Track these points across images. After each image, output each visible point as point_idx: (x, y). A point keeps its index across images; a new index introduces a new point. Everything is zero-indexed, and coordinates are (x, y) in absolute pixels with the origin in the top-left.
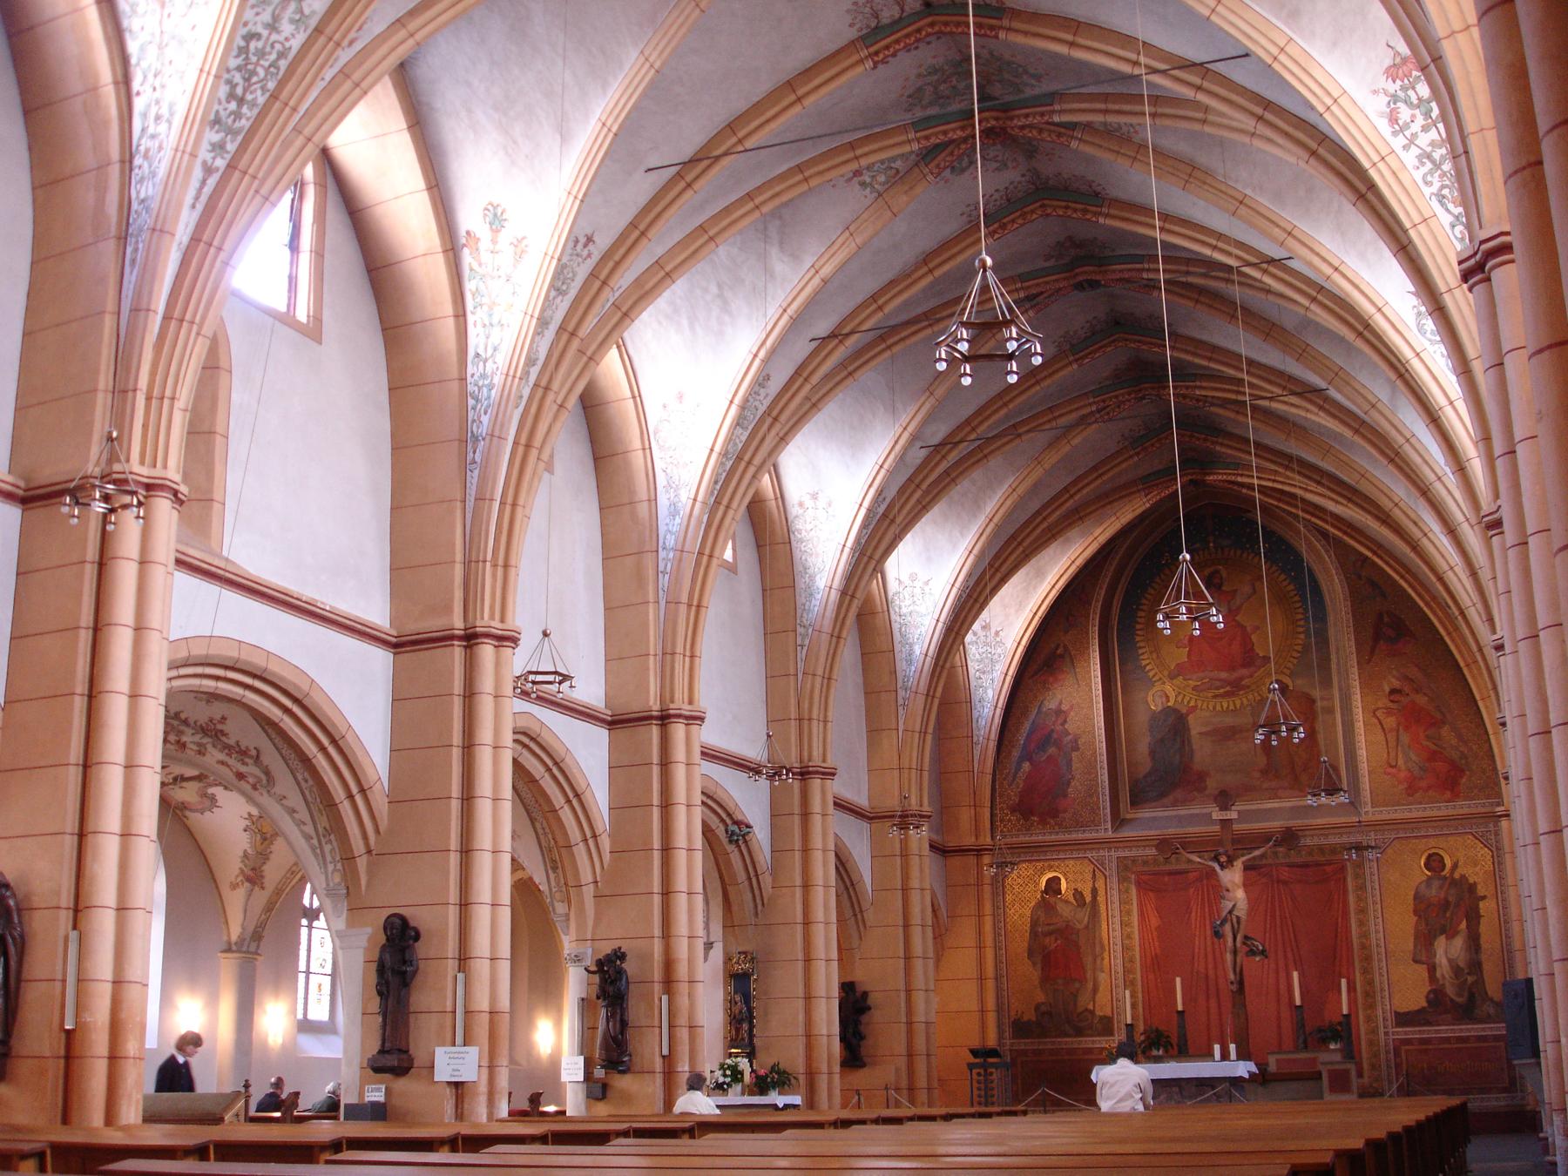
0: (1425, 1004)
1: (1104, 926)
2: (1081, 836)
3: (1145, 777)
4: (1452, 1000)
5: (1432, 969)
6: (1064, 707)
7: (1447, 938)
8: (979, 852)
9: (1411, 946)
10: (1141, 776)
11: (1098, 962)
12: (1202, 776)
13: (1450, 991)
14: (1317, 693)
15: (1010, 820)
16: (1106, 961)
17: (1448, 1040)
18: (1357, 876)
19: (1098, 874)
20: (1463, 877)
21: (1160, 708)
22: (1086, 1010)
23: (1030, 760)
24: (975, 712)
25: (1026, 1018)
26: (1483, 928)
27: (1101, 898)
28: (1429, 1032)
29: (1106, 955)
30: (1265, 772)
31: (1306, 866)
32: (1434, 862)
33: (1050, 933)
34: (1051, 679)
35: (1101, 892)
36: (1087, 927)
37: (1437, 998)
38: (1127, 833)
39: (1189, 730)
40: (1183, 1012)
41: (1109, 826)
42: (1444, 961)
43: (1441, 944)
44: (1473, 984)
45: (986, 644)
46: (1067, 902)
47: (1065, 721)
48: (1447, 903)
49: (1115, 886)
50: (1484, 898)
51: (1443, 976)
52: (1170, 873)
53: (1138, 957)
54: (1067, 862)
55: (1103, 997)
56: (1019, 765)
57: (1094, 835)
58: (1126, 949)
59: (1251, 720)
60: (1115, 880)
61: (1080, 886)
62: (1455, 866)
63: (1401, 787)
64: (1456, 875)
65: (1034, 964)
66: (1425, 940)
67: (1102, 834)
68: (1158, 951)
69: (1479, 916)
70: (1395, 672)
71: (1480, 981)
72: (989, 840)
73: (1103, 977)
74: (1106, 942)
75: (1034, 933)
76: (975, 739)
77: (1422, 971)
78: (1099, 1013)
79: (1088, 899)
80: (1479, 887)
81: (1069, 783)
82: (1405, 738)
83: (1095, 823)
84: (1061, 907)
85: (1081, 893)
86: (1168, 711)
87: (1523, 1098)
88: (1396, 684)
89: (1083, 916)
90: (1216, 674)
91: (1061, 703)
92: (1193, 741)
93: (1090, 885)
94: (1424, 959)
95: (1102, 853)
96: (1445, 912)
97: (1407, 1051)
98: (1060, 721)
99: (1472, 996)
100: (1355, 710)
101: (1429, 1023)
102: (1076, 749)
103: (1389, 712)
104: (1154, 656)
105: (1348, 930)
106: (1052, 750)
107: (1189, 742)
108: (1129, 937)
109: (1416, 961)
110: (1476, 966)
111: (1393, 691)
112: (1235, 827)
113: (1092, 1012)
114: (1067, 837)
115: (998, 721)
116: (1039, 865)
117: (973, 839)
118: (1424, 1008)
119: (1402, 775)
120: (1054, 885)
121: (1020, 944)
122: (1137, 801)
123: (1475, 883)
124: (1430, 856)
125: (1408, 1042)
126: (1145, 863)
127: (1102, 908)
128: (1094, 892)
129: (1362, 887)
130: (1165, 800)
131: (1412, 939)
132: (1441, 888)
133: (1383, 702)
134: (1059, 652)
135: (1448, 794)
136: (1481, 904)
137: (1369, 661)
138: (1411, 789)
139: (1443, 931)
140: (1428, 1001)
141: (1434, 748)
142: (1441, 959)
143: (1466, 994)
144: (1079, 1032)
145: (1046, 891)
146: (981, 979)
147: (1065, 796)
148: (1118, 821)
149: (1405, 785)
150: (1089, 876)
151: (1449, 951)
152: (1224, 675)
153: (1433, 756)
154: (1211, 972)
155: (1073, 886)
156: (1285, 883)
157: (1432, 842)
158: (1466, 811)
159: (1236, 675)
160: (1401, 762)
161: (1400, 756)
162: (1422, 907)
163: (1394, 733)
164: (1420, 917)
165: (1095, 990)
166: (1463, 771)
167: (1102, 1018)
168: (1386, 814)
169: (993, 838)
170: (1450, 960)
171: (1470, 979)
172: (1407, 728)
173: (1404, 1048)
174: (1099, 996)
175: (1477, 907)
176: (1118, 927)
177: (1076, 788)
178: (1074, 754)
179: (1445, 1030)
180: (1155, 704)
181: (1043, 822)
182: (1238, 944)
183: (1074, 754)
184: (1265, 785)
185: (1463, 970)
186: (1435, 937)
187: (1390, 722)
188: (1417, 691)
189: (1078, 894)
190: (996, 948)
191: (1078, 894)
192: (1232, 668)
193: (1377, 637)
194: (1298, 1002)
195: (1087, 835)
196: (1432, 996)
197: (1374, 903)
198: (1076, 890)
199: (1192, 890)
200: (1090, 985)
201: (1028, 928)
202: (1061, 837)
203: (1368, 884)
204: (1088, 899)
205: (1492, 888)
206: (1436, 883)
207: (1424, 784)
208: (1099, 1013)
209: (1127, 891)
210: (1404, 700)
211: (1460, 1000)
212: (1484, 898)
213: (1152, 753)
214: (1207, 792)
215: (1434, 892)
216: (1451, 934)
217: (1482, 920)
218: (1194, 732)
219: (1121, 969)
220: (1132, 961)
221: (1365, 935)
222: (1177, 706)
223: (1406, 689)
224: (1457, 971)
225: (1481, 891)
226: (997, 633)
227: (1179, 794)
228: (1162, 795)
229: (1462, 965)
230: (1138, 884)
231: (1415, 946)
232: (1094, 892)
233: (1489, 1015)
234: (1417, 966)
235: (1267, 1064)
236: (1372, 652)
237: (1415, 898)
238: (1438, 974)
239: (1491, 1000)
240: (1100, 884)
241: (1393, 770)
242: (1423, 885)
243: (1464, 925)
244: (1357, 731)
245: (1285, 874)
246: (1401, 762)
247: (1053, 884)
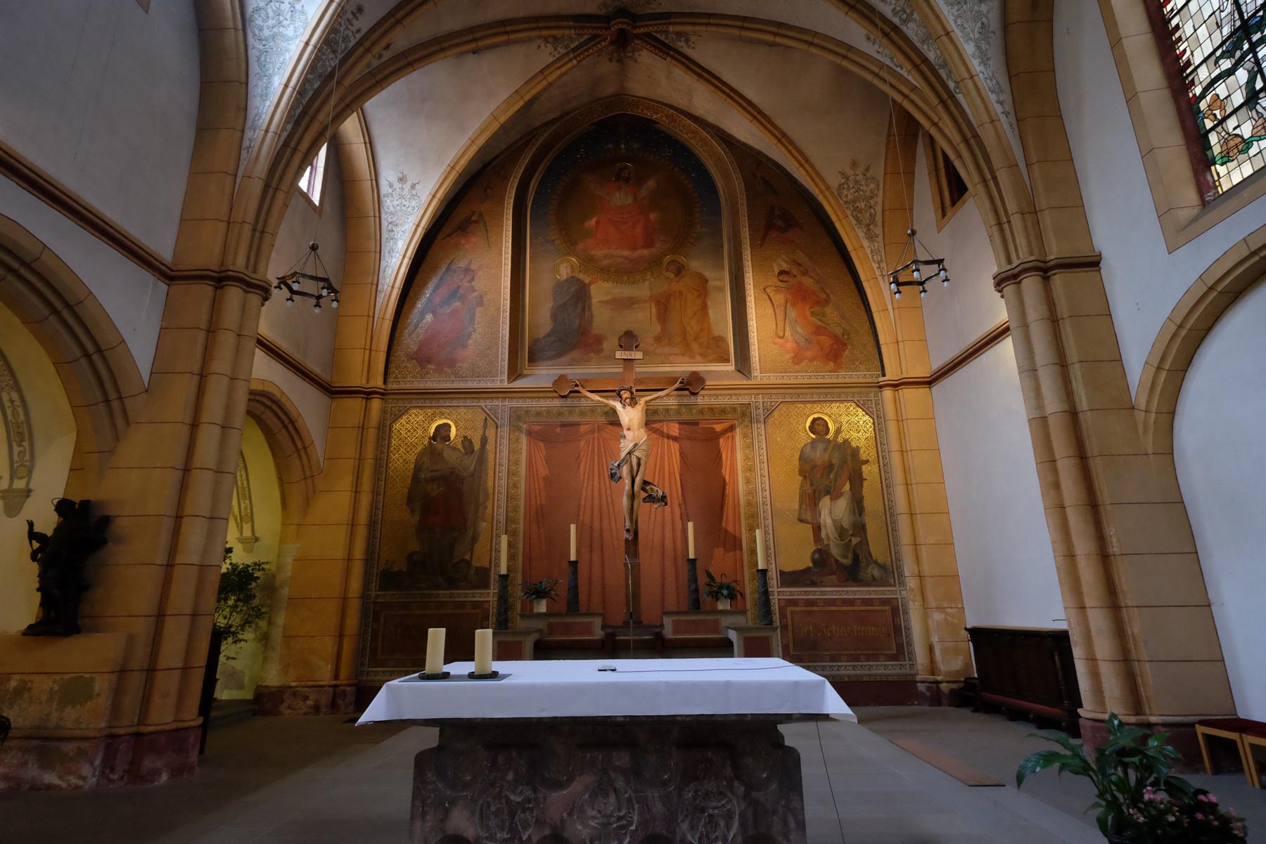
0: (811, 565)
1: (491, 473)
2: (475, 385)
3: (544, 337)
4: (837, 561)
5: (817, 529)
6: (473, 267)
7: (831, 499)
8: (368, 394)
9: (796, 505)
10: (541, 336)
11: (481, 511)
12: (599, 340)
13: (835, 551)
14: (707, 274)
15: (406, 367)
16: (489, 511)
17: (833, 602)
18: (745, 436)
19: (490, 422)
20: (846, 441)
21: (565, 277)
22: (463, 560)
23: (434, 312)
24: (383, 264)
25: (396, 569)
26: (867, 490)
27: (490, 447)
28: (814, 593)
29: (489, 504)
30: (658, 339)
31: (696, 424)
32: (818, 426)
33: (433, 480)
34: (463, 241)
35: (491, 441)
36: (472, 475)
37: (822, 559)
38: (519, 384)
39: (590, 297)
40: (694, 560)
41: (506, 378)
42: (829, 521)
43: (825, 502)
44: (856, 545)
45: (401, 197)
46: (454, 448)
47: (473, 279)
48: (830, 466)
49: (506, 435)
50: (867, 462)
51: (828, 538)
52: (563, 425)
53: (522, 506)
54: (459, 410)
55: (481, 548)
56: (423, 314)
57: (490, 385)
58: (510, 498)
59: (648, 293)
60: (506, 429)
61: (469, 434)
62: (838, 431)
63: (788, 356)
64: (840, 440)
65: (412, 511)
66: (811, 499)
67: (498, 385)
68: (544, 503)
69: (862, 479)
70: (784, 256)
71: (864, 542)
72: (378, 382)
73: (484, 525)
74: (491, 491)
75: (416, 479)
76: (380, 287)
77: (808, 530)
78: (475, 564)
79: (477, 447)
80: (862, 451)
81: (469, 336)
82: (792, 313)
83: (491, 374)
84: (448, 454)
85: (470, 442)
86: (572, 280)
87: (912, 666)
88: (785, 266)
89: (470, 463)
90: (619, 252)
91: (470, 262)
92: (593, 308)
93: (480, 432)
94: (809, 518)
95: (496, 403)
96: (830, 472)
97: (792, 612)
98: (468, 278)
99: (856, 558)
100: (747, 286)
101: (814, 584)
102: (480, 304)
103: (778, 289)
104: (564, 233)
105: (735, 483)
106: (457, 304)
107: (590, 308)
108: (515, 486)
109: (801, 521)
110: (860, 528)
111: (782, 273)
112: (639, 369)
113: (469, 563)
114: (462, 385)
115: (404, 270)
116: (430, 411)
117: (364, 381)
118: (808, 569)
119: (790, 345)
120: (443, 432)
121: (400, 488)
122: (533, 360)
123: (858, 448)
124: (814, 420)
125: (793, 603)
126: (538, 414)
127: (491, 456)
128: (484, 440)
129: (750, 446)
130: (562, 359)
131: (797, 498)
132: (825, 449)
133: (775, 281)
134: (474, 218)
135: (832, 364)
136: (864, 468)
137: (761, 245)
138: (797, 359)
139: (828, 493)
140: (814, 561)
141: (819, 323)
142: (826, 519)
143: (850, 555)
144: (453, 584)
145: (434, 438)
146: (353, 525)
147: (464, 346)
148: (514, 373)
149: (792, 355)
150: (479, 424)
151: (833, 512)
152: (626, 253)
153: (818, 330)
154: (596, 525)
155: (463, 433)
156: (675, 439)
157: (817, 407)
158: (848, 380)
159: (638, 253)
160: (788, 333)
161: (787, 330)
162: (807, 468)
163: (783, 308)
164: (805, 477)
165: (474, 539)
166: (846, 345)
167: (477, 569)
168: (773, 378)
169: (385, 382)
170: (834, 521)
171: (855, 541)
172: (794, 305)
173: (789, 609)
174: (477, 546)
175: (861, 469)
176: (504, 474)
177: (475, 341)
178: (479, 310)
179: (831, 592)
180: (564, 272)
181: (439, 370)
182: (636, 488)
183: (479, 310)
184: (659, 351)
185: (847, 530)
186: (820, 499)
187: (779, 298)
188: (805, 273)
189: (467, 441)
190: (375, 492)
191: (467, 441)
192: (634, 248)
193: (769, 226)
194: (692, 556)
195: (483, 385)
196: (817, 556)
197: (761, 462)
198: (465, 437)
199: (582, 443)
200: (470, 533)
201: (410, 474)
202: (456, 385)
203: (756, 443)
204: (477, 447)
205: (873, 452)
206: (821, 446)
207: (809, 354)
208: (475, 564)
209: (517, 440)
210: (792, 281)
211: (845, 561)
212: (867, 462)
213: (554, 316)
214: (603, 354)
215: (819, 455)
216: (834, 494)
217: (865, 483)
218: (594, 301)
219: (502, 519)
220: (515, 510)
221: (752, 493)
222: (581, 276)
223: (795, 271)
224: (841, 532)
225: (863, 457)
226: (413, 186)
227: (576, 354)
228: (559, 355)
229: (846, 525)
230: (530, 434)
231: (801, 505)
232: (484, 440)
233: (874, 578)
234: (802, 525)
235: (662, 626)
236: (764, 238)
237: (800, 459)
238: (823, 534)
239: (876, 562)
240: (491, 433)
241: (781, 341)
242: (809, 447)
243: (847, 487)
244: (748, 304)
245: (674, 429)
246: (788, 333)
247: (442, 431)
